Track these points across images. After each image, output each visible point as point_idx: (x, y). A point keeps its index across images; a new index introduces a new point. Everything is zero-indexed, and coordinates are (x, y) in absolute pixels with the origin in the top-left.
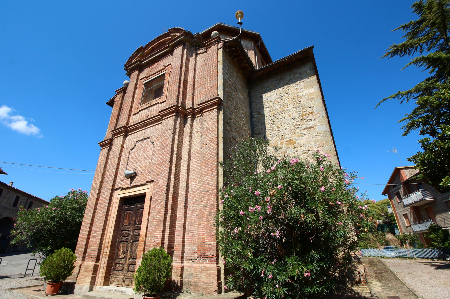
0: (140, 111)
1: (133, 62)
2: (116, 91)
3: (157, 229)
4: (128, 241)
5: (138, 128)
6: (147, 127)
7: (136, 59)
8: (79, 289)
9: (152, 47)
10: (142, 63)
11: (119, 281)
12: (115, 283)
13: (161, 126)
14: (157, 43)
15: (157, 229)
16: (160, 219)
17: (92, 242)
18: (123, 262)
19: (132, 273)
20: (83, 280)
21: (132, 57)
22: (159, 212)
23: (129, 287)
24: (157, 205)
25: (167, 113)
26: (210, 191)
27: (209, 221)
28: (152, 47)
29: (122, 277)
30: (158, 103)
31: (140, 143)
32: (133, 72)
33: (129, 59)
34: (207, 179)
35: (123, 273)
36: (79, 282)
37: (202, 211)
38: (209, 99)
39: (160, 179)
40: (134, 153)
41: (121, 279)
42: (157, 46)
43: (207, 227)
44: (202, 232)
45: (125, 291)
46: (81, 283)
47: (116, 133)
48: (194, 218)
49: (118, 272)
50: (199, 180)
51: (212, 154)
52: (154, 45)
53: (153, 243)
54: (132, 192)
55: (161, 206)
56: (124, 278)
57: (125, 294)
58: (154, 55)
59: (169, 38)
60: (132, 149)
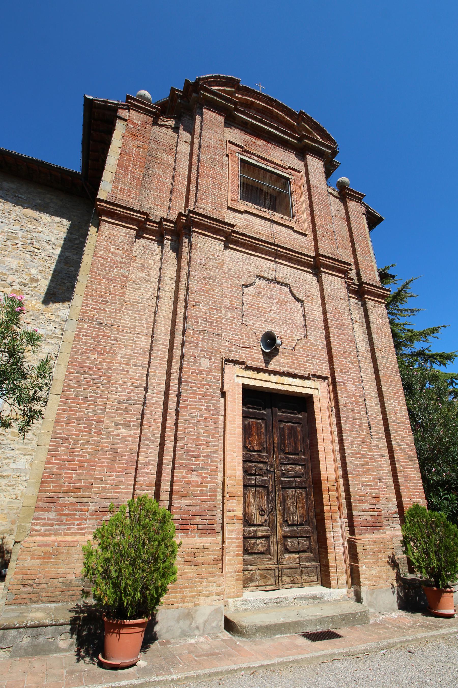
0: (246, 212)
1: (214, 88)
2: (128, 97)
3: (366, 471)
4: (268, 486)
5: (255, 249)
6: (277, 260)
7: (219, 90)
8: (178, 621)
9: (252, 100)
10: (237, 114)
11: (266, 577)
12: (254, 584)
13: (310, 277)
14: (264, 104)
15: (366, 471)
16: (368, 455)
17: (189, 482)
18: (265, 533)
19: (298, 556)
20: (191, 592)
21: (217, 81)
22: (362, 441)
23: (296, 586)
24: (354, 428)
25: (333, 266)
26: (402, 423)
27: (411, 468)
28: (252, 100)
29: (273, 567)
30: (292, 228)
31: (264, 283)
32: (210, 110)
33: (211, 77)
34: (395, 405)
35: (271, 559)
36: (175, 598)
37: (399, 451)
38: (371, 282)
39: (348, 381)
40: (253, 296)
41: (270, 572)
42: (249, 103)
43: (410, 477)
44: (405, 482)
45: (321, 594)
46: (184, 602)
47: (205, 224)
48: (379, 459)
49: (255, 557)
50: (374, 401)
51: (394, 370)
52: (257, 101)
53: (364, 496)
54: (275, 383)
55: (363, 432)
56: (278, 568)
57: (324, 602)
58: (266, 124)
59: (293, 122)
60: (246, 286)
